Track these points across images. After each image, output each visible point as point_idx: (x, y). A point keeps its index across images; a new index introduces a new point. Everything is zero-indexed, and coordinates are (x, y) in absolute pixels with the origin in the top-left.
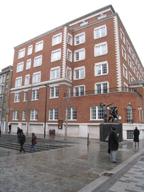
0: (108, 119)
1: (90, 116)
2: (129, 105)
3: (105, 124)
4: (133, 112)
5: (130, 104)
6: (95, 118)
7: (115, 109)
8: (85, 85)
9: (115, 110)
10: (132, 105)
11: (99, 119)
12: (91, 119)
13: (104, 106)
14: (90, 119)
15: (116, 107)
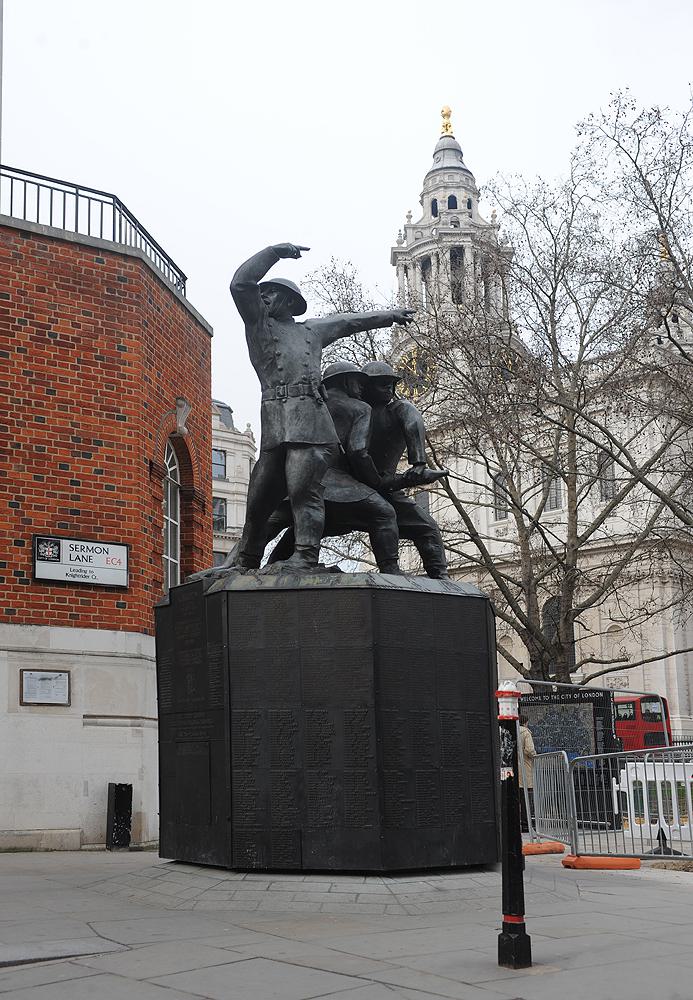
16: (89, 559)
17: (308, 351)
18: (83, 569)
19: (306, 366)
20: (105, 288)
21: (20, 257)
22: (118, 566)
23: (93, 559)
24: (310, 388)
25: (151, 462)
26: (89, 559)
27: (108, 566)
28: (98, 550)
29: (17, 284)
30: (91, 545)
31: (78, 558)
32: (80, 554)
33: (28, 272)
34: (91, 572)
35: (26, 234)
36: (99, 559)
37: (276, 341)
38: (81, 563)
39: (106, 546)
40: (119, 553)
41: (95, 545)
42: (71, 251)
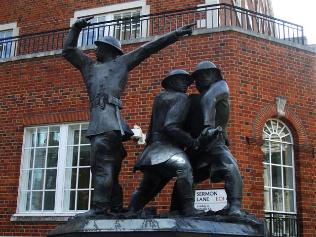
0: (132, 183)
1: (14, 189)
2: (275, 116)
3: (105, 225)
4: (298, 165)
5: (281, 112)
6: (50, 205)
7: (203, 88)
8: (20, 22)
9: (211, 95)
10: (297, 122)
11: (72, 208)
12: (23, 211)
13: (101, 60)
14: (13, 206)
15: (217, 75)
16: (206, 199)
17: (106, 75)
18: (204, 205)
19: (102, 86)
20: (214, 52)
21: (173, 51)
22: (222, 201)
23: (209, 199)
24: (99, 100)
25: (247, 138)
26: (206, 199)
27: (219, 201)
28: (212, 194)
29: (172, 65)
30: (207, 191)
31: (201, 199)
32: (202, 197)
33: (177, 57)
34: (208, 206)
35: (208, 35)
36: (212, 198)
37: (91, 76)
38: (203, 202)
39: (216, 191)
40: (222, 193)
41: (210, 191)
42: (197, 40)
